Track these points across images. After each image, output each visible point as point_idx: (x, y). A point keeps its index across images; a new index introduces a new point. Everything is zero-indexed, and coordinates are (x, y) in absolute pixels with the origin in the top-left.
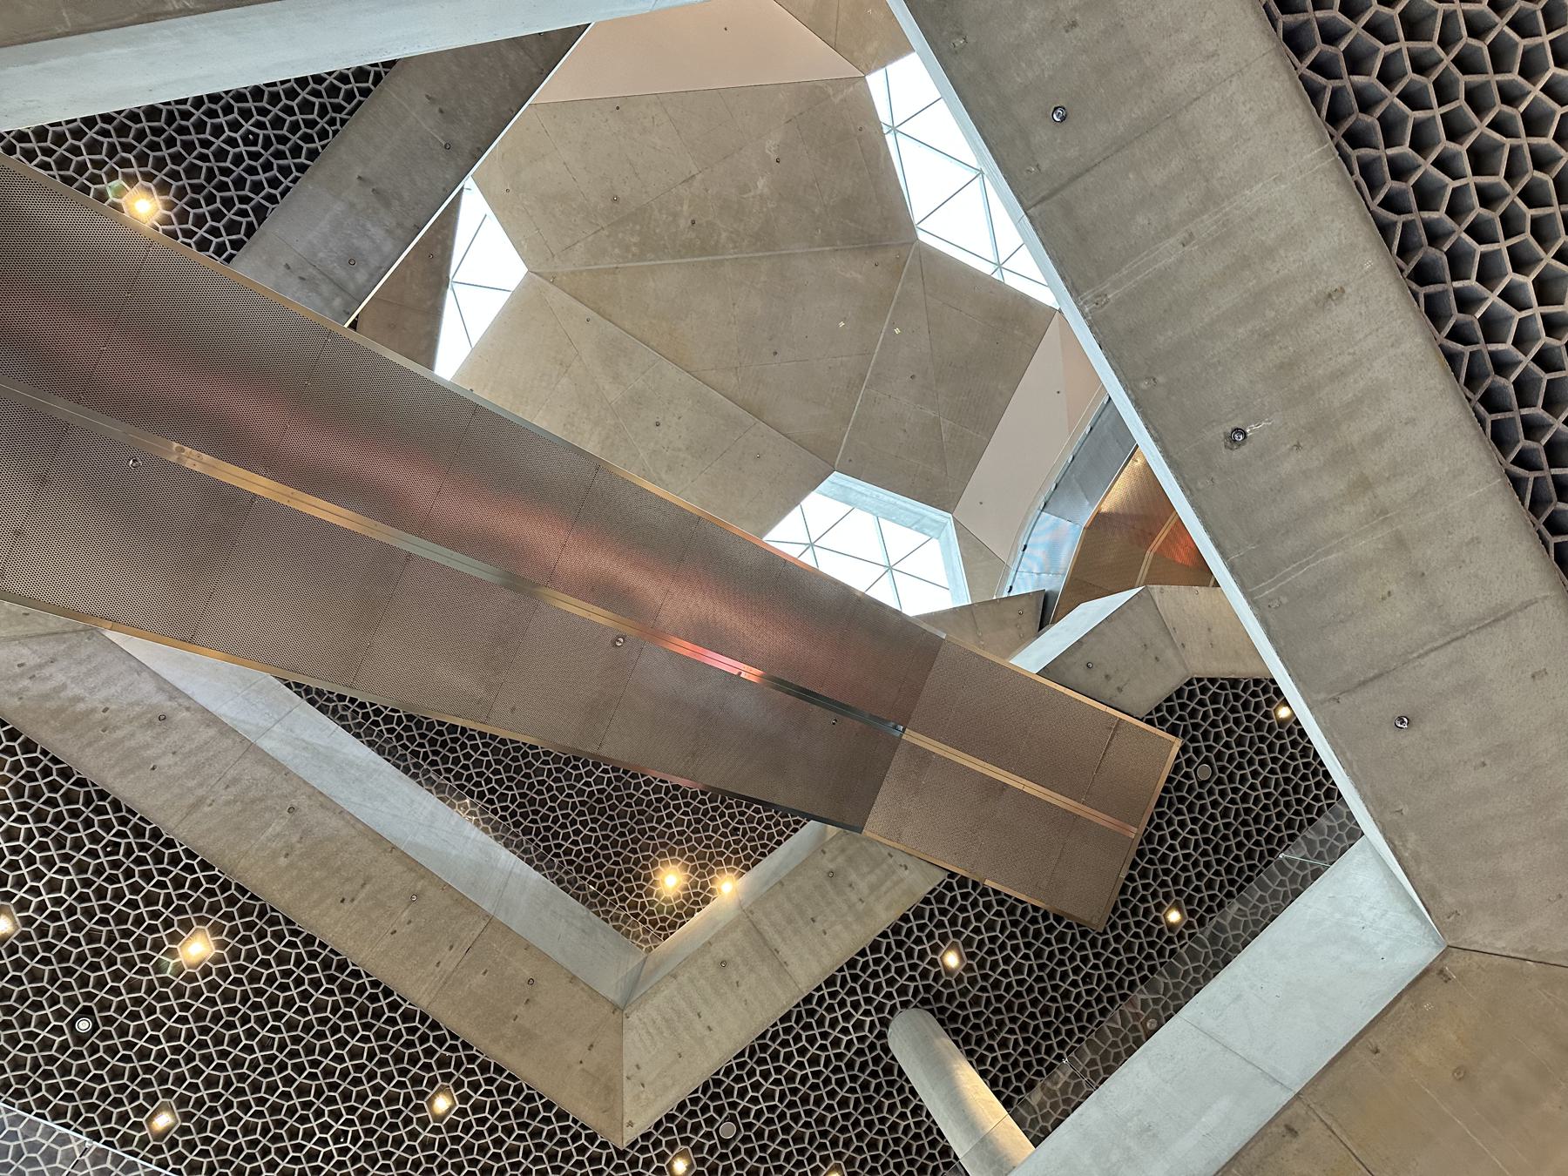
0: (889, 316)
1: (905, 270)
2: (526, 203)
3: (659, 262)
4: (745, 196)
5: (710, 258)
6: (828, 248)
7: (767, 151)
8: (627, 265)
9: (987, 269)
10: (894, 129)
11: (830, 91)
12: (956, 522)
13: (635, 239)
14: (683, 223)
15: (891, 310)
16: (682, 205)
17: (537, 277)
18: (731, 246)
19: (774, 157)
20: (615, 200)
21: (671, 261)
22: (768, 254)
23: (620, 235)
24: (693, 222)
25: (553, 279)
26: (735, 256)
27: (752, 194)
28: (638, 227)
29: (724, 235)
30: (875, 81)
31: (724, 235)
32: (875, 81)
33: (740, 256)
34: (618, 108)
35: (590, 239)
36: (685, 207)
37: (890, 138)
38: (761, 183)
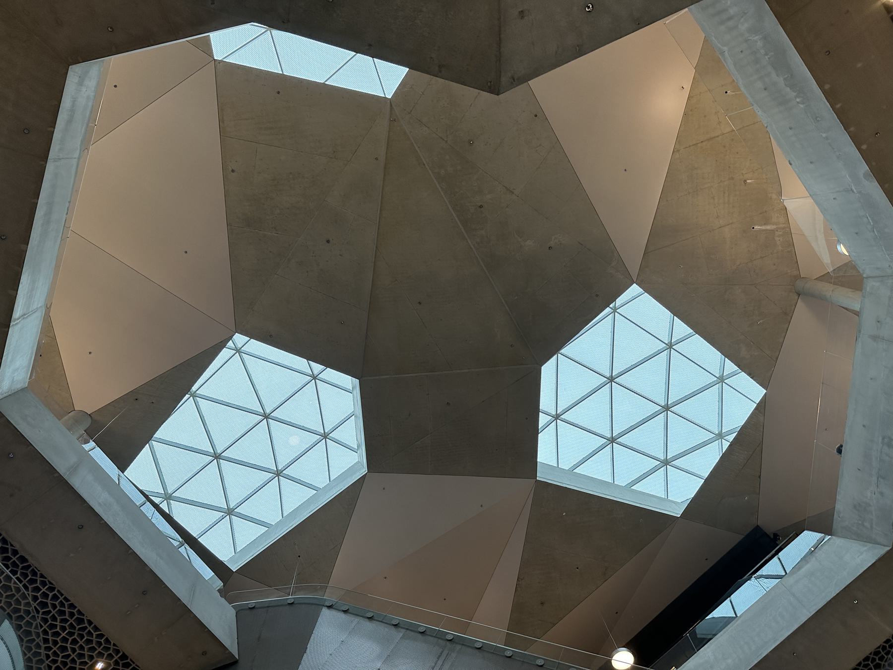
3: (442, 194)
5: (463, 230)
6: (507, 308)
7: (553, 238)
8: (430, 171)
10: (615, 310)
12: (363, 478)
20: (470, 143)
21: (447, 202)
22: (484, 268)
24: (481, 207)
25: (393, 120)
26: (472, 247)
30: (635, 289)
32: (635, 289)
33: (474, 249)
37: (608, 310)
38: (529, 243)
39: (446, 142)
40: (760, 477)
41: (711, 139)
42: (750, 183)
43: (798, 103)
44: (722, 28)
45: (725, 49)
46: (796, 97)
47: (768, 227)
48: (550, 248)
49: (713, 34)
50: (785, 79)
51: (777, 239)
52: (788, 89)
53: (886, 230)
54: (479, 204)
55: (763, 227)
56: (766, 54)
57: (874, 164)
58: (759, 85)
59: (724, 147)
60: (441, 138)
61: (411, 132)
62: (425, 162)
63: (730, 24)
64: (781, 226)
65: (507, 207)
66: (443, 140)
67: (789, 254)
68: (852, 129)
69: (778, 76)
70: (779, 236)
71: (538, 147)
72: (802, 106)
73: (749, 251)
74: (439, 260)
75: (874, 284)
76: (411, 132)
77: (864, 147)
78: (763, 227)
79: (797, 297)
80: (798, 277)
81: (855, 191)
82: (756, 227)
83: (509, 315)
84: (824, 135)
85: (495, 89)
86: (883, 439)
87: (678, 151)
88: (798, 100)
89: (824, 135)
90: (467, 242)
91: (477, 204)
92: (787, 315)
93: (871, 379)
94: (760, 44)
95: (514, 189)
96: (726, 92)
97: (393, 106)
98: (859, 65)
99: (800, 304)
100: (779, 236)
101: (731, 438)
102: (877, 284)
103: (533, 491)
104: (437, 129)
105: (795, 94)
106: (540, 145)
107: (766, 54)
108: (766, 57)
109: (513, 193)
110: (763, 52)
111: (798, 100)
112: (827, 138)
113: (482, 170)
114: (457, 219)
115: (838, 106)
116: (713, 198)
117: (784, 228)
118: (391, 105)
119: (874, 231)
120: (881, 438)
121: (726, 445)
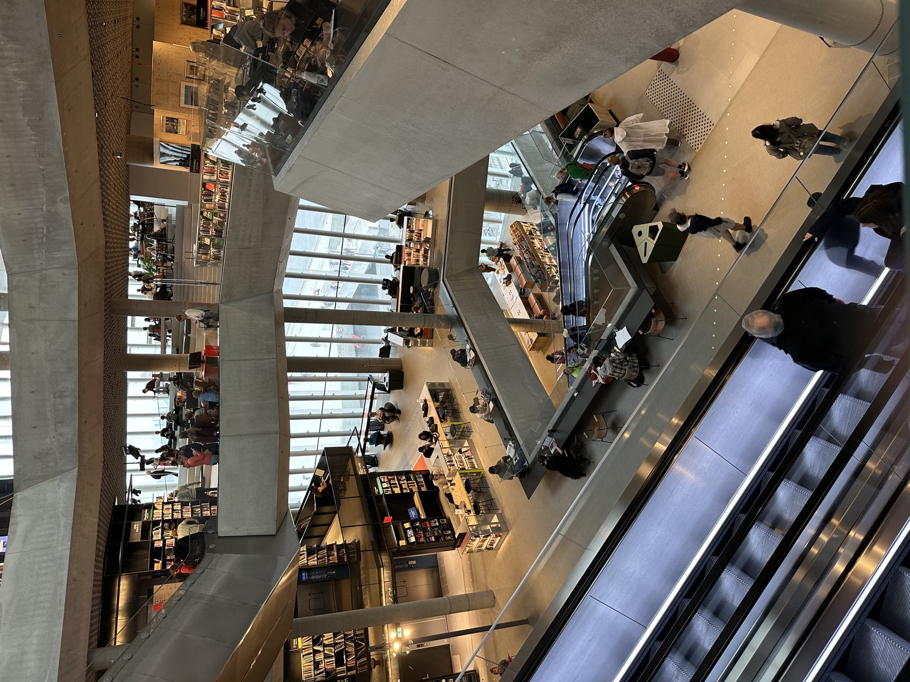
43: (32, 140)
56: (23, 97)
69: (24, 116)
75: (20, 278)
81: (45, 209)
84: (41, 167)
88: (33, 138)
89: (41, 167)
93: (33, 353)
102: (24, 278)
105: (33, 133)
107: (23, 97)
108: (22, 99)
111: (33, 138)
112: (44, 170)
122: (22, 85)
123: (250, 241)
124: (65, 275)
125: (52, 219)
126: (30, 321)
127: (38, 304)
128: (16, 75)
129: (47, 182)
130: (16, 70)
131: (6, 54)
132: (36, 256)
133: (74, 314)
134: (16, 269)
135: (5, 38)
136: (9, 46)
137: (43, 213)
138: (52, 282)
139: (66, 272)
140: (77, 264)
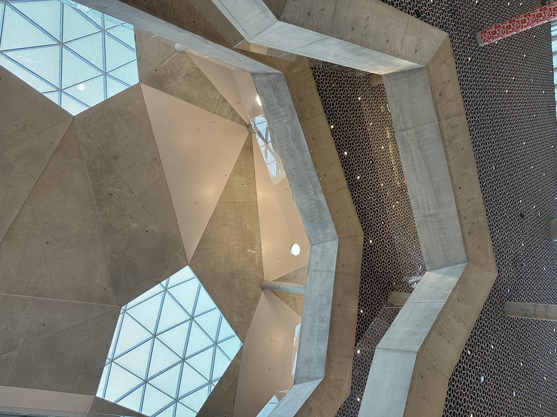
0: (79, 302)
1: (105, 305)
2: (107, 117)
4: (129, 218)
6: (110, 262)
7: (150, 226)
8: (85, 163)
9: (110, 356)
11: (179, 251)
13: (98, 167)
14: (110, 189)
15: (83, 302)
16: (119, 188)
17: (72, 120)
18: (103, 213)
19: (148, 229)
20: (116, 158)
23: (99, 160)
26: (98, 216)
27: (130, 221)
28: (104, 168)
29: (108, 209)
31: (108, 209)
32: (186, 272)
34: (156, 159)
35: (95, 146)
36: (118, 190)
39: (101, 152)
40: (234, 402)
41: (234, 202)
42: (248, 228)
43: (300, 157)
44: (276, 121)
45: (275, 130)
46: (299, 154)
47: (253, 252)
48: (147, 231)
49: (271, 123)
50: (296, 146)
51: (256, 258)
52: (297, 150)
53: (324, 218)
54: (111, 192)
55: (251, 251)
56: (291, 134)
57: (323, 187)
58: (285, 148)
59: (239, 208)
60: (98, 148)
61: (81, 138)
62: (83, 157)
63: (280, 119)
64: (259, 253)
65: (127, 200)
66: (100, 150)
67: (260, 268)
68: (318, 170)
70: (257, 257)
71: (153, 175)
72: (301, 158)
73: (244, 261)
74: (73, 217)
76: (81, 138)
77: (321, 179)
78: (251, 251)
79: (262, 291)
80: (262, 280)
81: (314, 199)
82: (248, 250)
83: (110, 267)
84: (307, 172)
85: (278, 17)
86: (320, 319)
87: (220, 203)
88: (300, 156)
89: (307, 172)
90: (96, 212)
91: (109, 192)
92: (256, 299)
94: (290, 129)
95: (134, 192)
96: (243, 184)
97: (74, 120)
98: (322, 147)
99: (263, 297)
100: (257, 257)
101: (216, 383)
102: (316, 247)
103: (91, 404)
104: (98, 143)
105: (299, 153)
106: (155, 174)
107: (291, 134)
108: (291, 135)
109: (133, 193)
110: (290, 133)
111: (300, 156)
112: (308, 174)
113: (118, 175)
114: (93, 196)
115: (314, 160)
116: (232, 230)
117: (259, 254)
118: (73, 120)
119: (318, 219)
120: (318, 319)
121: (213, 388)
122: (289, 127)
123: (429, 209)
124: (332, 245)
125: (318, 204)
126: (315, 271)
127: (320, 262)
128: (287, 123)
129: (311, 181)
130: (286, 121)
131: (282, 114)
132: (319, 231)
133: (333, 268)
134: (313, 242)
135: (280, 107)
136: (282, 110)
137: (315, 201)
138: (327, 249)
139: (333, 243)
140: (338, 238)
